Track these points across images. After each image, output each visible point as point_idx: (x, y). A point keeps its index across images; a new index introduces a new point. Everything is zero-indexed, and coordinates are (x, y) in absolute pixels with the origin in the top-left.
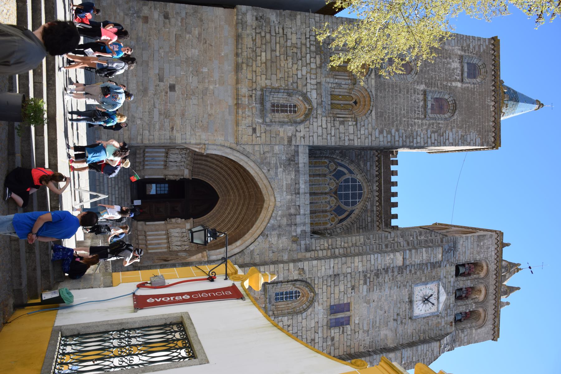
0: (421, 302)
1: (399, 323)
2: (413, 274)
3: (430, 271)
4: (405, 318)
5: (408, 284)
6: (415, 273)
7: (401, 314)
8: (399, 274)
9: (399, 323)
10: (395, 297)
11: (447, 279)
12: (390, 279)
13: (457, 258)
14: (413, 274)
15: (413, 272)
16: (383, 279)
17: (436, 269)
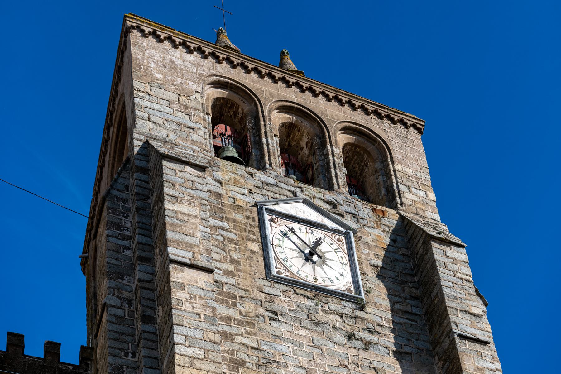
0: (318, 269)
1: (375, 338)
2: (238, 270)
3: (232, 224)
4: (363, 319)
5: (266, 290)
6: (233, 261)
7: (349, 329)
8: (234, 304)
9: (375, 338)
10: (303, 332)
11: (257, 190)
12: (248, 333)
13: (199, 149)
14: (238, 270)
15: (231, 268)
16: (249, 352)
17: (226, 209)
